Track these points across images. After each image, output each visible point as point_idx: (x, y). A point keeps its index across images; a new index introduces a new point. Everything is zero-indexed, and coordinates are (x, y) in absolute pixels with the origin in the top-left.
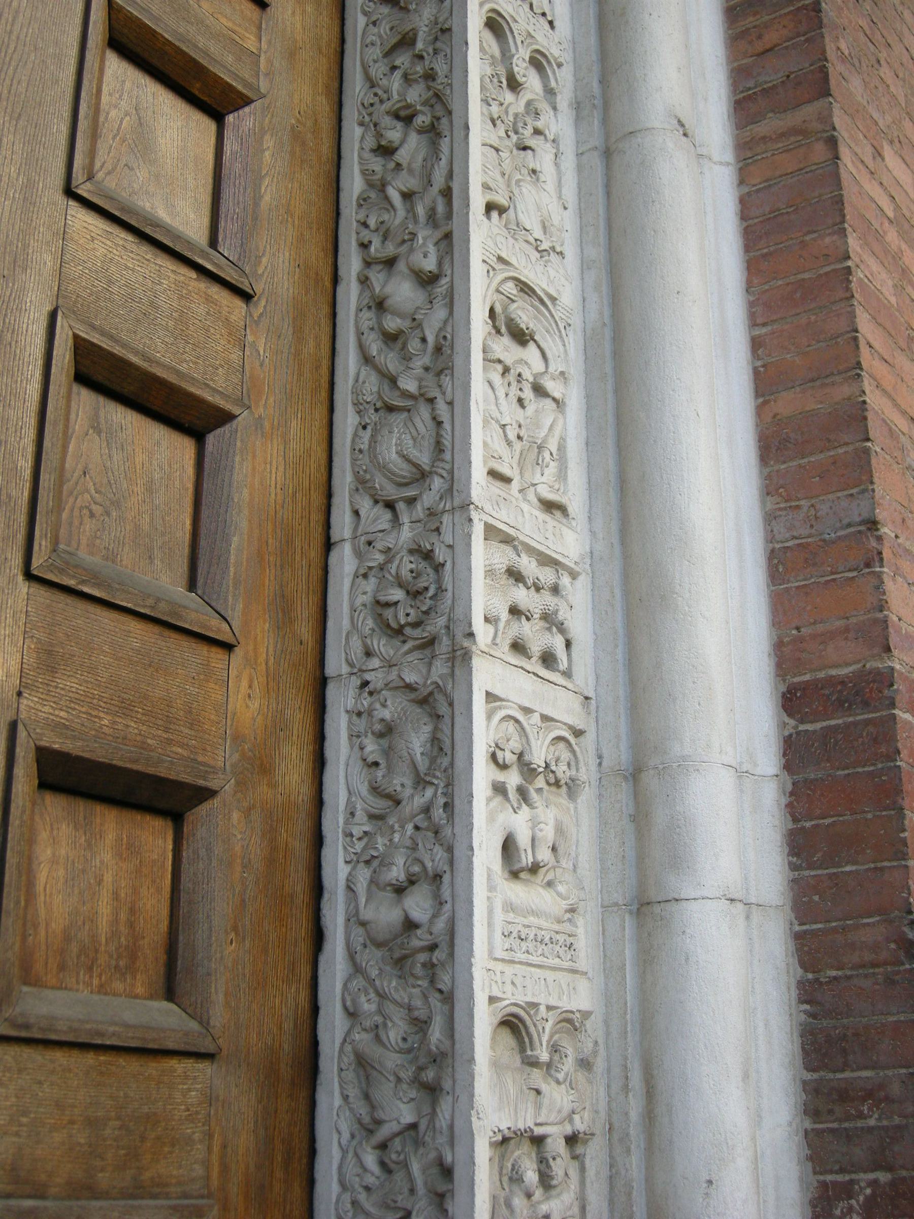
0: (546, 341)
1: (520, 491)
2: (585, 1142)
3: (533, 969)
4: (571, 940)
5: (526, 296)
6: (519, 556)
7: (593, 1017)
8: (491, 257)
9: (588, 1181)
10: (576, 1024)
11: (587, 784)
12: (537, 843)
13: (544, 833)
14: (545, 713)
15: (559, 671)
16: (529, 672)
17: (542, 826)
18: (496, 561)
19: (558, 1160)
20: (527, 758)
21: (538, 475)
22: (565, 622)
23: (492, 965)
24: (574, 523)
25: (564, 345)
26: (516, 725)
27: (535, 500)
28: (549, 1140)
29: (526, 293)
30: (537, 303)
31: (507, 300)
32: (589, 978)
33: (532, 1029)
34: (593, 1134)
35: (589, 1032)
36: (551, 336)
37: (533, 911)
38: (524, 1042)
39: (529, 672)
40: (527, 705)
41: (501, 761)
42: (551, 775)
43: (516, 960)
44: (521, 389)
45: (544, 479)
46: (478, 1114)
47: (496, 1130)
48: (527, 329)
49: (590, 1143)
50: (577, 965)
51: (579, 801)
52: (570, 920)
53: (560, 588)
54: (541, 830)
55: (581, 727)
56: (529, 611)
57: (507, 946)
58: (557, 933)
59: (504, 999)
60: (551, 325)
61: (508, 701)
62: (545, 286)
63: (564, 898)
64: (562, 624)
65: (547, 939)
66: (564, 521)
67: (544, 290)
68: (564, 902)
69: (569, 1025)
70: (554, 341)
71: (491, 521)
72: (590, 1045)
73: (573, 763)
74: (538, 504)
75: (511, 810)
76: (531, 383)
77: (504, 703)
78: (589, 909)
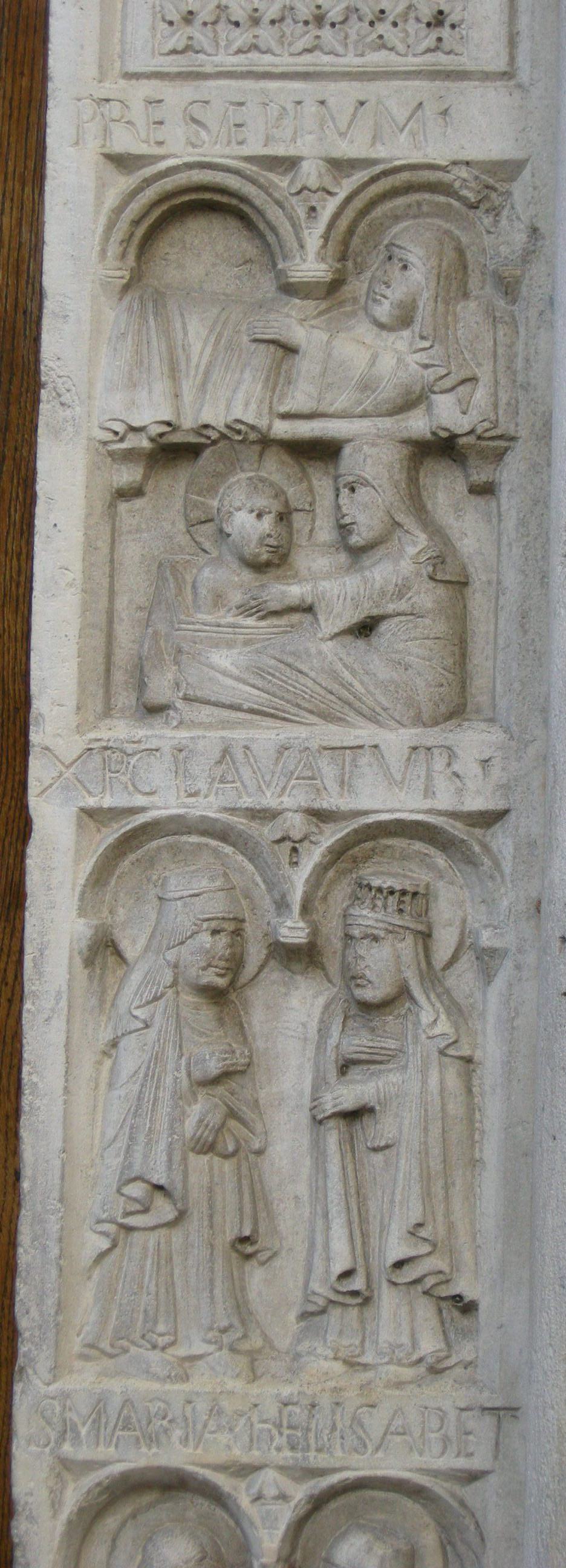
2: (499, 456)
3: (273, 85)
7: (526, 173)
9: (505, 540)
10: (465, 192)
19: (362, 492)
23: (112, 88)
28: (347, 451)
32: (519, 86)
33: (274, 213)
34: (513, 439)
35: (519, 208)
38: (269, 245)
43: (208, 69)
46: (59, 395)
47: (120, 428)
49: (509, 458)
50: (463, 59)
57: (177, 40)
59: (163, 158)
65: (335, 14)
69: (442, 199)
72: (520, 238)
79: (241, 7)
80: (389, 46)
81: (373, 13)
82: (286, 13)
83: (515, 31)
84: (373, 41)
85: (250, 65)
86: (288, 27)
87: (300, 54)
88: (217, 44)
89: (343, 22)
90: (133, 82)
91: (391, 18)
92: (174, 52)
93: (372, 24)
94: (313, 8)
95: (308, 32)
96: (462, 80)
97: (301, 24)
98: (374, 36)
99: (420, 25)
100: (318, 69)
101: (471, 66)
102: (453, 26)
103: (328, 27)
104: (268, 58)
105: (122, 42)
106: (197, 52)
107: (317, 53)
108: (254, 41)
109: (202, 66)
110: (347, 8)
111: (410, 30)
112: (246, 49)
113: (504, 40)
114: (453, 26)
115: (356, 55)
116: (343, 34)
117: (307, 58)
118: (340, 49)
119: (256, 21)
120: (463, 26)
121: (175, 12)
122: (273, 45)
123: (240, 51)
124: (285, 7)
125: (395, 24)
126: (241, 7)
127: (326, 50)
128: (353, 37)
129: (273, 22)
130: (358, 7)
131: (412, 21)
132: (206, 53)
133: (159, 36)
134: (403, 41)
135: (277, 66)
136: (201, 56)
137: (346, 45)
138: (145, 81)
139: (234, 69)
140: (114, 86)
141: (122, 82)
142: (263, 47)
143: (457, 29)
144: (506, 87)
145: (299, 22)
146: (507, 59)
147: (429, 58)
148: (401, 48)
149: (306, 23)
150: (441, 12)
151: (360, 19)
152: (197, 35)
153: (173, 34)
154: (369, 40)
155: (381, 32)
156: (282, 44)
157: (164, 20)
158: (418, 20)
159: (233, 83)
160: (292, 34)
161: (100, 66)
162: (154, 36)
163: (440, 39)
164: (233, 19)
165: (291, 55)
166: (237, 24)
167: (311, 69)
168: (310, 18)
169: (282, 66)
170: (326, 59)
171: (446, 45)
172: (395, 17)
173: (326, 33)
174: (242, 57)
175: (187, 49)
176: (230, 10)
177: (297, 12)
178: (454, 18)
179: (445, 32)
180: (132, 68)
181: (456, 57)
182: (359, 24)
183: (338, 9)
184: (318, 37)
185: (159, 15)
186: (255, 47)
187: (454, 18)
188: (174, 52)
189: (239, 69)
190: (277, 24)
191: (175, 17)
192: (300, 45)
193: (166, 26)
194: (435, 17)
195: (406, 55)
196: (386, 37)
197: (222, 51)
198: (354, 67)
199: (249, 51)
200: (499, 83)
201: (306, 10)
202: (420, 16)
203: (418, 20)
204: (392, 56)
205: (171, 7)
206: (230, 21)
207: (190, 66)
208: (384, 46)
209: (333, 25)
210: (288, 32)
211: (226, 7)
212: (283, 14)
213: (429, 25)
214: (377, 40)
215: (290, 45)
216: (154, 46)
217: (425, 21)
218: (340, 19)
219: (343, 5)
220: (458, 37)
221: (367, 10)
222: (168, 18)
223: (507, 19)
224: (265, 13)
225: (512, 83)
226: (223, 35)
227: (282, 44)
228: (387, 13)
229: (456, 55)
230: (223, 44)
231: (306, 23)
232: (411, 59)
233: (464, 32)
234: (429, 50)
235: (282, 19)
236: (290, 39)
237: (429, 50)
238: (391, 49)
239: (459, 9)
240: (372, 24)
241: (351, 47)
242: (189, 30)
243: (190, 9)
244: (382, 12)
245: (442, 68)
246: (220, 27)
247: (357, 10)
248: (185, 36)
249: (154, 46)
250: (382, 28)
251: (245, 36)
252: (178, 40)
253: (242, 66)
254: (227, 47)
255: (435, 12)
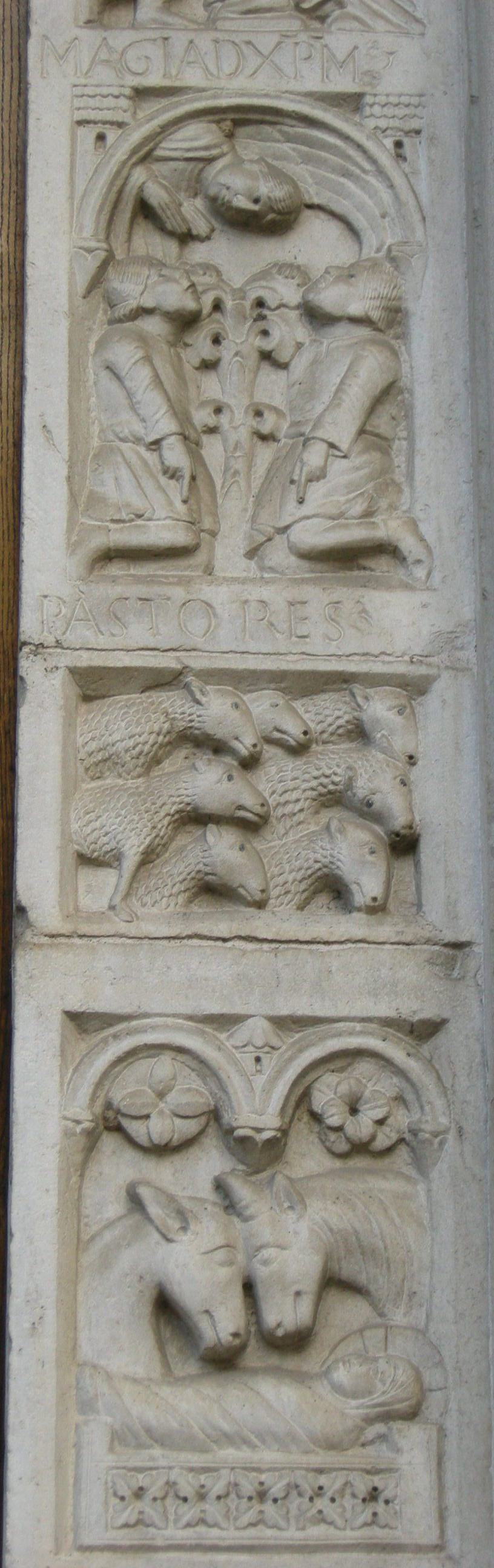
0: (348, 196)
1: (252, 553)
4: (377, 1481)
5: (267, 129)
6: (198, 702)
8: (110, 102)
11: (451, 1137)
12: (261, 1290)
13: (274, 1266)
14: (285, 1012)
15: (359, 910)
16: (225, 940)
17: (266, 1253)
18: (116, 737)
20: (227, 1118)
21: (291, 505)
22: (377, 799)
24: (420, 572)
25: (391, 186)
26: (181, 1057)
27: (293, 560)
29: (262, 122)
30: (302, 130)
31: (192, 165)
32: (450, 1558)
36: (356, 179)
37: (226, 1435)
39: (225, 940)
40: (215, 1009)
41: (143, 1140)
42: (333, 1136)
43: (159, 1542)
44: (265, 333)
45: (306, 509)
48: (256, 201)
50: (398, 1533)
51: (434, 1174)
52: (382, 1438)
53: (368, 727)
54: (266, 1262)
55: (428, 1012)
56: (240, 807)
57: (129, 1514)
58: (320, 1471)
60: (348, 158)
61: (146, 1015)
62: (313, 83)
63: (354, 1395)
64: (369, 805)
65: (277, 1490)
66: (401, 573)
67: (310, 95)
68: (354, 1403)
70: (365, 186)
71: (85, 660)
73: (410, 1097)
74: (305, 564)
75: (156, 1236)
76: (298, 307)
77: (134, 1023)
78: (453, 1405)
79: (189, 1483)
80: (329, 1520)
81: (313, 1490)
82: (231, 1489)
83: (443, 1507)
84: (313, 1516)
85: (199, 1539)
86: (232, 1502)
87: (245, 1528)
88: (167, 1519)
89: (285, 1498)
90: (87, 1554)
91: (329, 1494)
92: (126, 1526)
93: (311, 1499)
94: (256, 1485)
95: (252, 1507)
96: (397, 1552)
97: (245, 1500)
98: (314, 1511)
99: (356, 1501)
100: (263, 1542)
101: (405, 1540)
102: (387, 1502)
103: (270, 1502)
104: (215, 1532)
105: (76, 1516)
106: (148, 1526)
107: (260, 1527)
108: (202, 1515)
109: (153, 1539)
110: (288, 1484)
111: (346, 1505)
112: (194, 1523)
113: (435, 1515)
114: (387, 1502)
115: (298, 1529)
116: (285, 1510)
117: (252, 1532)
118: (282, 1523)
119: (202, 1497)
120: (396, 1502)
121: (126, 1488)
122: (220, 1519)
123: (188, 1525)
124: (230, 1483)
125: (333, 1500)
126: (189, 1483)
127: (270, 1523)
128: (294, 1511)
129: (219, 1498)
130: (299, 1483)
131: (348, 1496)
132: (155, 1527)
133: (111, 1510)
134: (342, 1515)
135: (224, 1539)
136: (152, 1530)
137: (288, 1520)
138: (98, 1554)
139: (184, 1542)
140: (68, 1558)
141: (77, 1555)
142: (210, 1520)
143: (391, 1504)
144: (438, 1558)
145: (243, 1498)
146: (438, 1532)
147: (366, 1532)
148: (340, 1522)
149: (250, 1498)
150: (375, 1489)
151: (300, 1495)
152: (147, 1510)
153: (126, 1508)
154: (309, 1514)
155: (320, 1508)
156: (228, 1519)
157: (115, 1494)
158: (354, 1496)
159: (184, 1556)
160: (237, 1509)
161: (56, 1539)
162: (107, 1511)
163: (375, 1514)
164: (182, 1494)
165: (237, 1529)
166: (185, 1500)
167: (256, 1542)
168: (254, 1494)
169: (229, 1539)
170: (269, 1532)
171: (382, 1519)
172: (334, 1494)
173: (269, 1508)
174: (190, 1532)
175: (139, 1522)
176: (177, 1487)
177: (242, 1489)
178: (387, 1494)
179: (380, 1507)
180: (87, 1540)
181: (391, 1531)
182: (299, 1500)
183: (279, 1485)
184: (261, 1512)
185: (111, 1491)
186: (202, 1521)
187: (387, 1494)
188: (126, 1526)
189: (189, 1542)
190: (222, 1500)
191: (127, 1493)
192: (245, 1519)
193: (118, 1501)
194: (370, 1494)
195: (344, 1529)
196: (325, 1512)
197: (171, 1524)
198: (297, 1540)
199: (197, 1524)
200: (431, 1555)
201: (250, 1487)
202: (356, 1492)
203: (354, 1496)
204: (332, 1530)
205: (123, 1483)
206: (177, 1496)
207: (143, 1539)
208: (324, 1521)
209: (275, 1500)
210: (233, 1507)
211: (175, 1483)
212: (228, 1489)
213: (364, 1500)
214: (317, 1515)
215: (236, 1519)
216: (107, 1521)
217: (361, 1496)
218: (282, 1495)
219: (285, 1482)
220: (392, 1512)
221: (308, 1488)
222: (120, 1493)
223: (436, 1496)
224: (212, 1489)
225: (443, 1555)
226: (171, 1510)
227: (228, 1519)
228: (325, 1488)
229: (391, 1528)
230: (172, 1518)
231: (250, 1498)
232: (349, 1533)
233: (397, 1508)
234: (366, 1524)
235: (227, 1495)
236: (235, 1513)
237: (366, 1524)
238: (331, 1523)
239: (392, 1485)
240: (311, 1499)
241: (293, 1521)
242: (139, 1505)
243: (140, 1485)
244: (321, 1488)
245: (379, 1541)
246: (169, 1501)
247: (297, 1486)
248: (136, 1511)
249: (107, 1521)
250: (322, 1503)
251: (192, 1512)
252: (129, 1516)
253: (191, 1539)
254: (176, 1521)
255: (370, 1489)
